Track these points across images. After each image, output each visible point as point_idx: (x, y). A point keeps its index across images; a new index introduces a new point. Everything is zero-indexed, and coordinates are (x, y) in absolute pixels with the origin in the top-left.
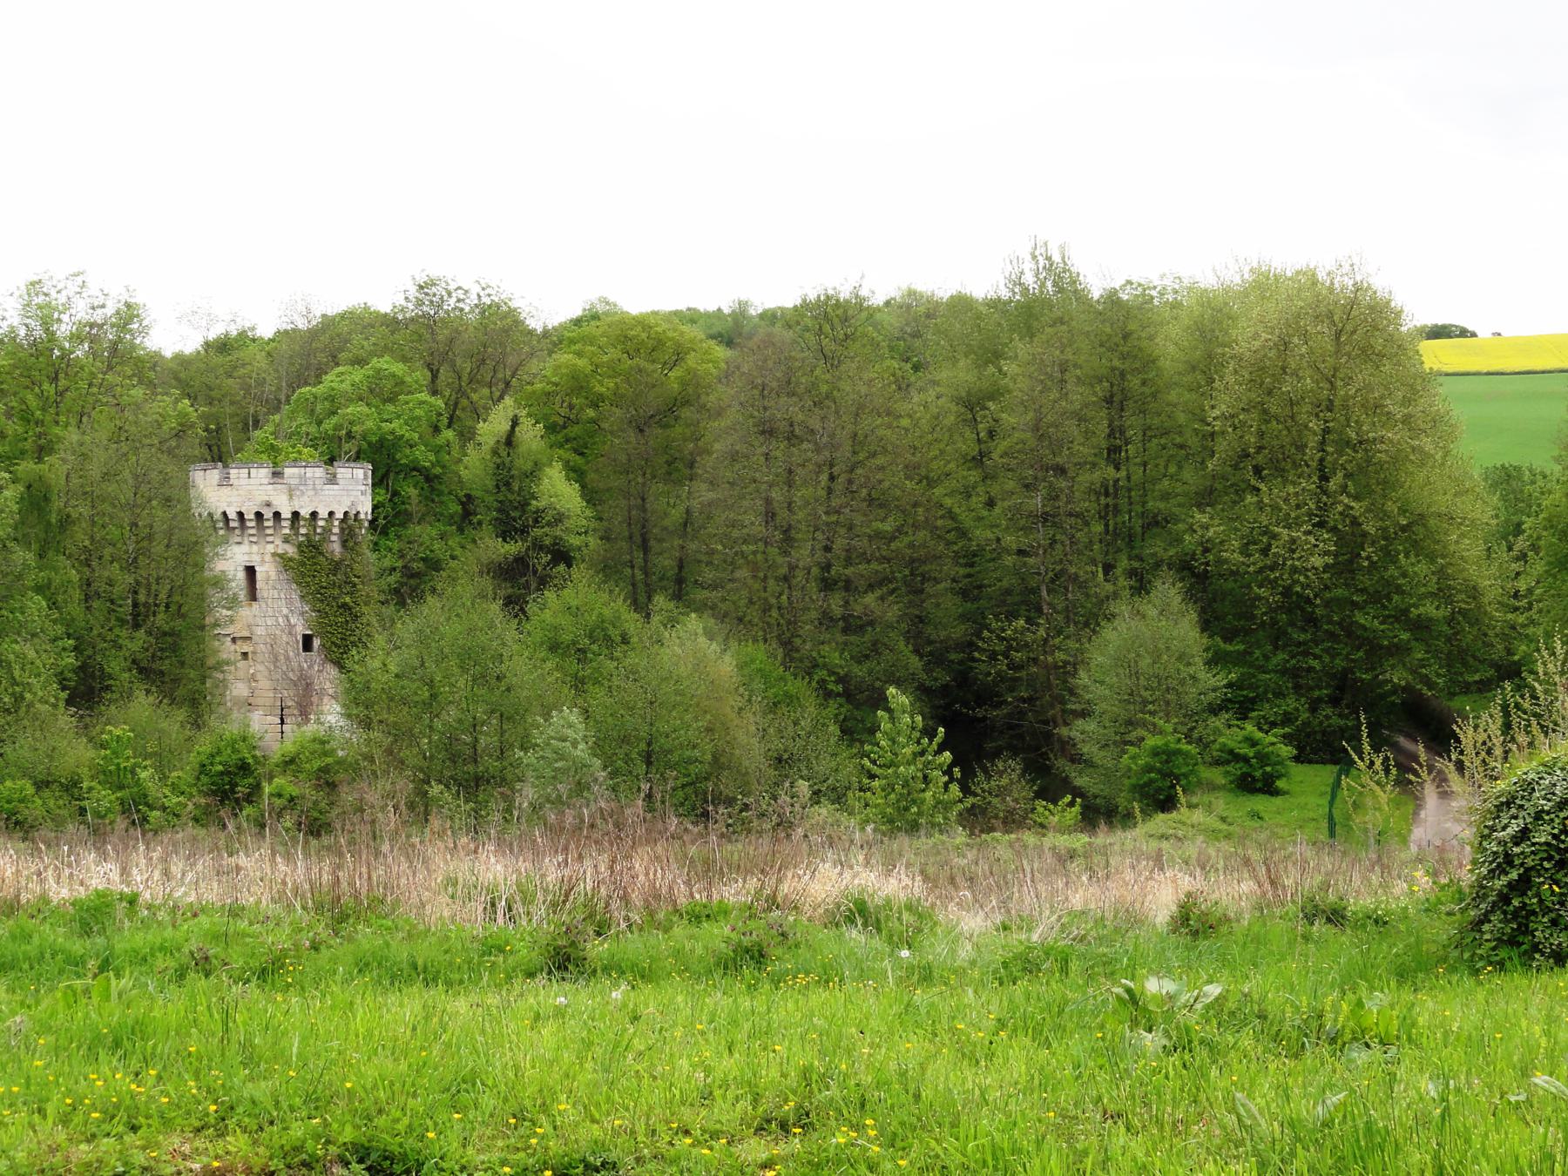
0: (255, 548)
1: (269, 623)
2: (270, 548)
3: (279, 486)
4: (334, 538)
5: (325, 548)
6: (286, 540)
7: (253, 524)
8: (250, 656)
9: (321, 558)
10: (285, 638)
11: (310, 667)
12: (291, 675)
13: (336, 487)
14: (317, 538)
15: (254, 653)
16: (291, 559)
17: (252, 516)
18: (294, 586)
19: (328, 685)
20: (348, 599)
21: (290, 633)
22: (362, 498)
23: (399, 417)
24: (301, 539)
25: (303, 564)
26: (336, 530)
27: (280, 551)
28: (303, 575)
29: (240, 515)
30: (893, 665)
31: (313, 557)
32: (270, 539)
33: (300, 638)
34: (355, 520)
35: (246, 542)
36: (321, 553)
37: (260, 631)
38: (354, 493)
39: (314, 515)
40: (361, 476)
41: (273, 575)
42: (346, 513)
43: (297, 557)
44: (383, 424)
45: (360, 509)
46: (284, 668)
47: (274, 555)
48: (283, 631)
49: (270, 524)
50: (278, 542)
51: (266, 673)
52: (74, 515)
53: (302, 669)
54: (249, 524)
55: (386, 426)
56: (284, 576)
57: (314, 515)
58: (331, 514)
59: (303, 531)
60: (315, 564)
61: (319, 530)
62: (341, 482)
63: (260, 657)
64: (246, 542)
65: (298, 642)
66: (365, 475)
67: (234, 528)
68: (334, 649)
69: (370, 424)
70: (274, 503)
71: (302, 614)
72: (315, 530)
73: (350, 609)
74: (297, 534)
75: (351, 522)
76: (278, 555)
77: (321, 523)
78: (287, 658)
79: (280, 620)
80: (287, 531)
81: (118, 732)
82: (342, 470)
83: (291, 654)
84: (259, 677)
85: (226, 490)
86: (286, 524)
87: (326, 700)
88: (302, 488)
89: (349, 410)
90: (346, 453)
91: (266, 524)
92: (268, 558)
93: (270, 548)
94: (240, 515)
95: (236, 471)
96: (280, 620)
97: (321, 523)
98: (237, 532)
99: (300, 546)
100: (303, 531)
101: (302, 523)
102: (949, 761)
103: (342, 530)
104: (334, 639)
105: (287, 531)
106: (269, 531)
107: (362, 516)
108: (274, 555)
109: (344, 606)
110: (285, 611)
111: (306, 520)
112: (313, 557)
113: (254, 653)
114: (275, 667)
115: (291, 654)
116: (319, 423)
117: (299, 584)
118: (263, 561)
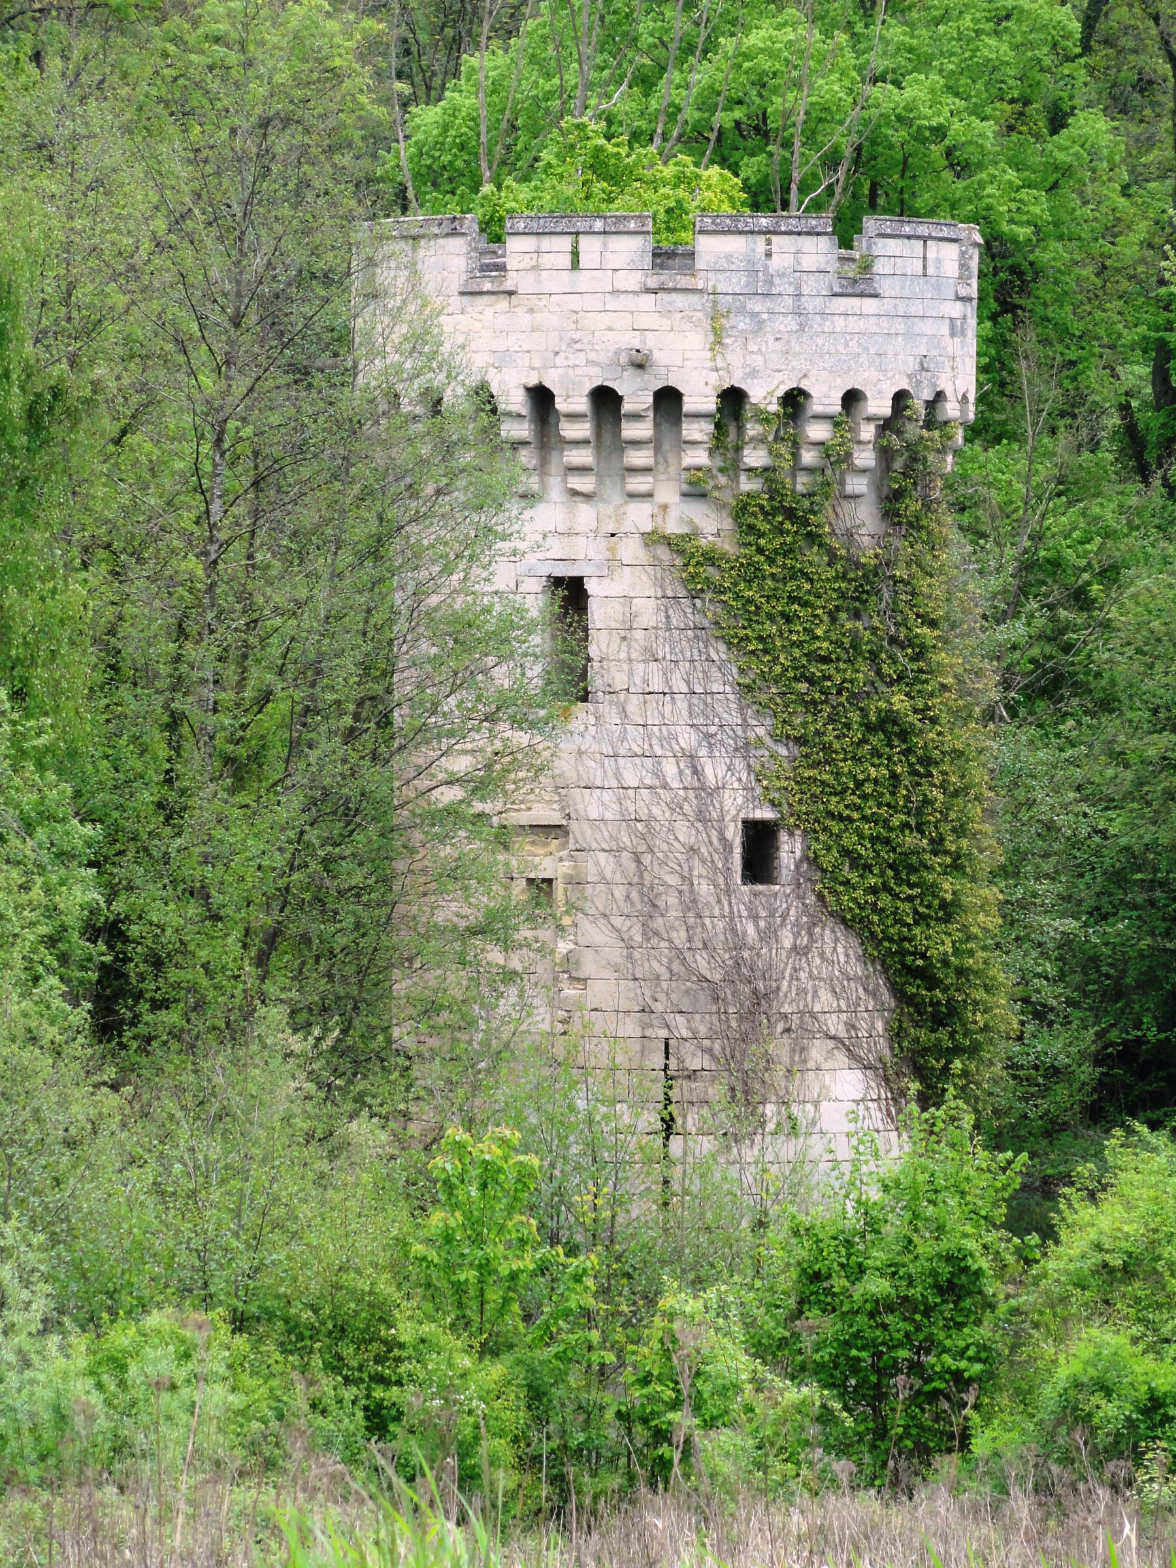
0: (586, 514)
1: (631, 780)
2: (640, 516)
3: (679, 300)
4: (858, 485)
5: (825, 521)
6: (696, 492)
7: (583, 430)
8: (559, 889)
9: (813, 555)
10: (683, 831)
11: (769, 935)
12: (701, 962)
13: (869, 305)
14: (803, 483)
15: (576, 882)
16: (710, 558)
17: (582, 404)
18: (719, 652)
19: (826, 1000)
20: (899, 702)
21: (701, 816)
22: (952, 346)
23: (923, 63)
24: (747, 485)
25: (751, 572)
26: (865, 457)
27: (673, 527)
28: (751, 612)
29: (541, 397)
30: (961, 972)
31: (788, 552)
32: (639, 484)
33: (735, 835)
34: (929, 424)
35: (555, 491)
36: (813, 538)
37: (592, 806)
38: (928, 327)
39: (794, 400)
40: (951, 269)
41: (648, 612)
42: (900, 398)
43: (728, 547)
44: (876, 92)
45: (944, 384)
46: (679, 937)
47: (653, 539)
48: (675, 807)
49: (642, 430)
50: (668, 493)
51: (617, 955)
52: (78, 389)
53: (738, 944)
54: (570, 430)
55: (885, 96)
56: (684, 615)
57: (794, 400)
58: (852, 398)
59: (755, 457)
60: (794, 574)
61: (808, 457)
62: (885, 286)
63: (597, 898)
64: (555, 491)
65: (727, 847)
66: (964, 266)
67: (517, 445)
68: (847, 873)
69: (830, 88)
70: (659, 357)
71: (745, 748)
72: (796, 456)
73: (904, 735)
74: (733, 468)
75: (913, 430)
76: (668, 541)
77: (817, 431)
78: (691, 904)
79: (670, 769)
80: (699, 457)
81: (488, 1150)
82: (893, 246)
83: (704, 889)
84: (589, 966)
85: (489, 311)
86: (698, 431)
87: (817, 1050)
88: (755, 305)
89: (755, 39)
90: (804, 189)
91: (630, 430)
92: (632, 550)
93: (640, 516)
94: (541, 397)
95: (528, 243)
96: (670, 769)
97: (817, 431)
98: (526, 457)
99: (741, 510)
100: (755, 457)
101: (753, 429)
102: (666, 1399)
103: (885, 454)
104: (850, 840)
105: (699, 457)
106: (639, 458)
107: (951, 409)
108: (653, 539)
109: (888, 724)
110: (687, 738)
111: (764, 418)
112: (788, 552)
113: (576, 882)
114: (649, 933)
115: (704, 889)
116: (646, 82)
117: (735, 643)
118: (614, 563)
